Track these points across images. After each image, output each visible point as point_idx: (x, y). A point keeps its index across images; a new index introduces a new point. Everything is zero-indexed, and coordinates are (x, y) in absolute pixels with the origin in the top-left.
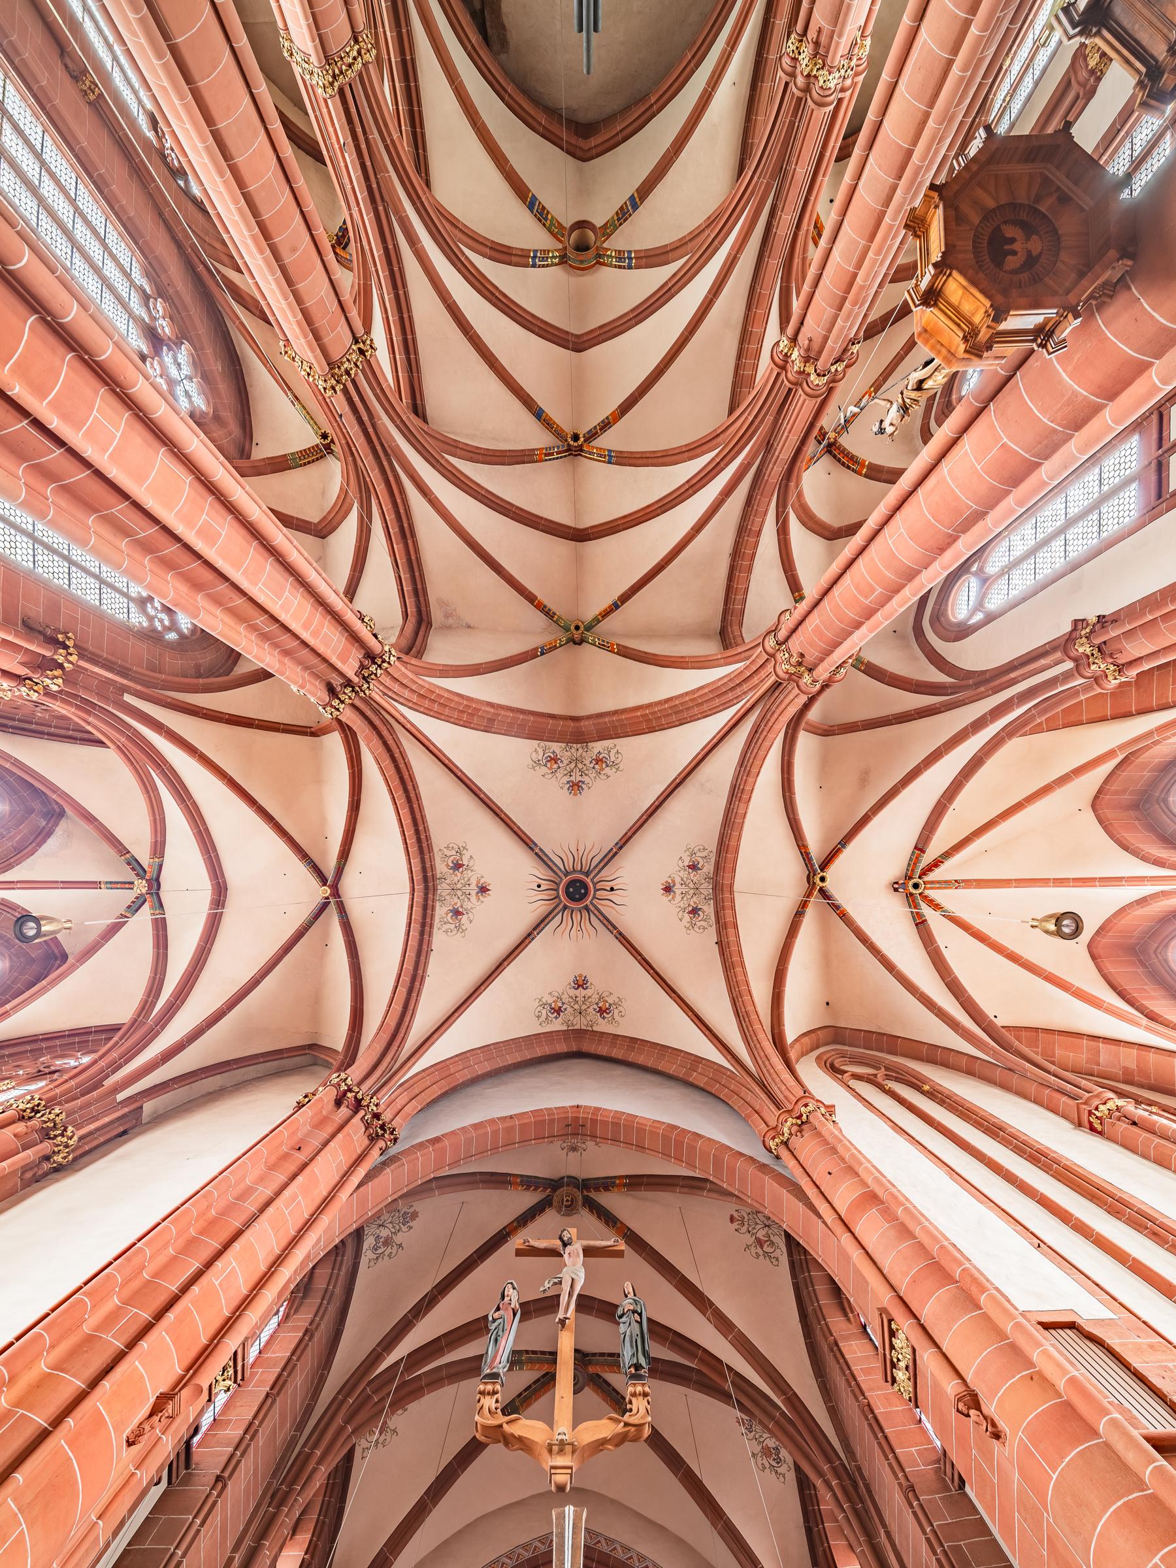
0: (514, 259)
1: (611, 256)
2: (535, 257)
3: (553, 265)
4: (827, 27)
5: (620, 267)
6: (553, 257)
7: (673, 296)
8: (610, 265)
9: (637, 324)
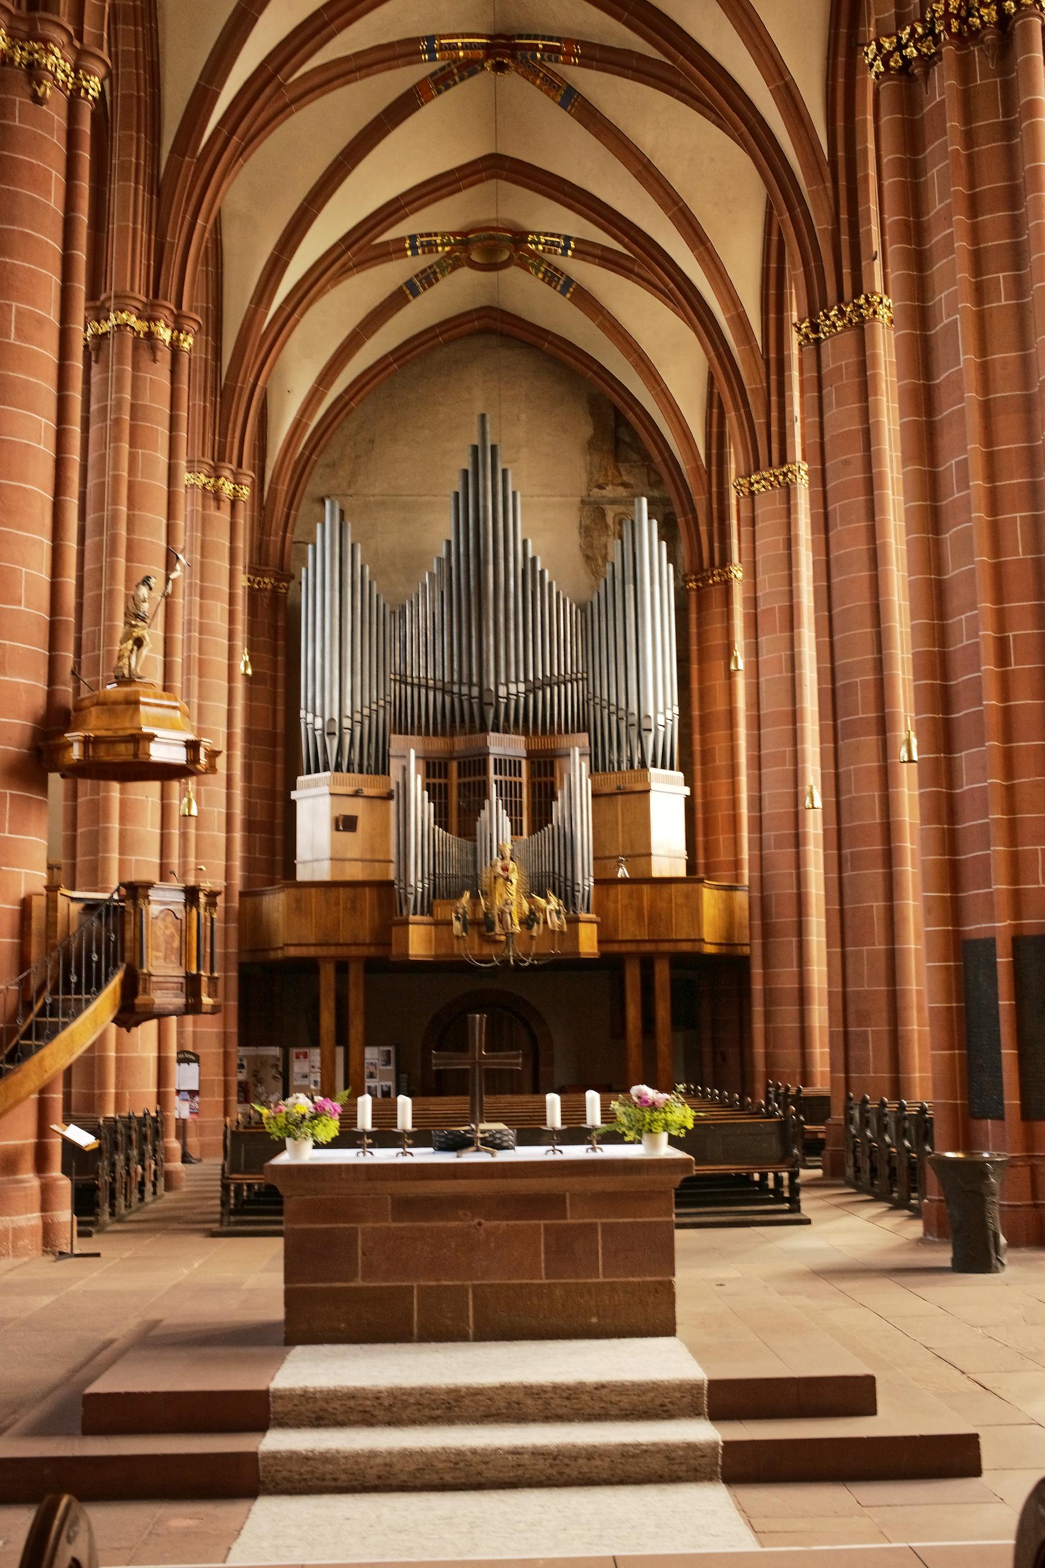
0: (599, 252)
1: (443, 245)
2: (566, 248)
3: (538, 234)
4: (212, 511)
5: (429, 235)
6: (537, 243)
7: (343, 239)
8: (443, 235)
9: (396, 199)
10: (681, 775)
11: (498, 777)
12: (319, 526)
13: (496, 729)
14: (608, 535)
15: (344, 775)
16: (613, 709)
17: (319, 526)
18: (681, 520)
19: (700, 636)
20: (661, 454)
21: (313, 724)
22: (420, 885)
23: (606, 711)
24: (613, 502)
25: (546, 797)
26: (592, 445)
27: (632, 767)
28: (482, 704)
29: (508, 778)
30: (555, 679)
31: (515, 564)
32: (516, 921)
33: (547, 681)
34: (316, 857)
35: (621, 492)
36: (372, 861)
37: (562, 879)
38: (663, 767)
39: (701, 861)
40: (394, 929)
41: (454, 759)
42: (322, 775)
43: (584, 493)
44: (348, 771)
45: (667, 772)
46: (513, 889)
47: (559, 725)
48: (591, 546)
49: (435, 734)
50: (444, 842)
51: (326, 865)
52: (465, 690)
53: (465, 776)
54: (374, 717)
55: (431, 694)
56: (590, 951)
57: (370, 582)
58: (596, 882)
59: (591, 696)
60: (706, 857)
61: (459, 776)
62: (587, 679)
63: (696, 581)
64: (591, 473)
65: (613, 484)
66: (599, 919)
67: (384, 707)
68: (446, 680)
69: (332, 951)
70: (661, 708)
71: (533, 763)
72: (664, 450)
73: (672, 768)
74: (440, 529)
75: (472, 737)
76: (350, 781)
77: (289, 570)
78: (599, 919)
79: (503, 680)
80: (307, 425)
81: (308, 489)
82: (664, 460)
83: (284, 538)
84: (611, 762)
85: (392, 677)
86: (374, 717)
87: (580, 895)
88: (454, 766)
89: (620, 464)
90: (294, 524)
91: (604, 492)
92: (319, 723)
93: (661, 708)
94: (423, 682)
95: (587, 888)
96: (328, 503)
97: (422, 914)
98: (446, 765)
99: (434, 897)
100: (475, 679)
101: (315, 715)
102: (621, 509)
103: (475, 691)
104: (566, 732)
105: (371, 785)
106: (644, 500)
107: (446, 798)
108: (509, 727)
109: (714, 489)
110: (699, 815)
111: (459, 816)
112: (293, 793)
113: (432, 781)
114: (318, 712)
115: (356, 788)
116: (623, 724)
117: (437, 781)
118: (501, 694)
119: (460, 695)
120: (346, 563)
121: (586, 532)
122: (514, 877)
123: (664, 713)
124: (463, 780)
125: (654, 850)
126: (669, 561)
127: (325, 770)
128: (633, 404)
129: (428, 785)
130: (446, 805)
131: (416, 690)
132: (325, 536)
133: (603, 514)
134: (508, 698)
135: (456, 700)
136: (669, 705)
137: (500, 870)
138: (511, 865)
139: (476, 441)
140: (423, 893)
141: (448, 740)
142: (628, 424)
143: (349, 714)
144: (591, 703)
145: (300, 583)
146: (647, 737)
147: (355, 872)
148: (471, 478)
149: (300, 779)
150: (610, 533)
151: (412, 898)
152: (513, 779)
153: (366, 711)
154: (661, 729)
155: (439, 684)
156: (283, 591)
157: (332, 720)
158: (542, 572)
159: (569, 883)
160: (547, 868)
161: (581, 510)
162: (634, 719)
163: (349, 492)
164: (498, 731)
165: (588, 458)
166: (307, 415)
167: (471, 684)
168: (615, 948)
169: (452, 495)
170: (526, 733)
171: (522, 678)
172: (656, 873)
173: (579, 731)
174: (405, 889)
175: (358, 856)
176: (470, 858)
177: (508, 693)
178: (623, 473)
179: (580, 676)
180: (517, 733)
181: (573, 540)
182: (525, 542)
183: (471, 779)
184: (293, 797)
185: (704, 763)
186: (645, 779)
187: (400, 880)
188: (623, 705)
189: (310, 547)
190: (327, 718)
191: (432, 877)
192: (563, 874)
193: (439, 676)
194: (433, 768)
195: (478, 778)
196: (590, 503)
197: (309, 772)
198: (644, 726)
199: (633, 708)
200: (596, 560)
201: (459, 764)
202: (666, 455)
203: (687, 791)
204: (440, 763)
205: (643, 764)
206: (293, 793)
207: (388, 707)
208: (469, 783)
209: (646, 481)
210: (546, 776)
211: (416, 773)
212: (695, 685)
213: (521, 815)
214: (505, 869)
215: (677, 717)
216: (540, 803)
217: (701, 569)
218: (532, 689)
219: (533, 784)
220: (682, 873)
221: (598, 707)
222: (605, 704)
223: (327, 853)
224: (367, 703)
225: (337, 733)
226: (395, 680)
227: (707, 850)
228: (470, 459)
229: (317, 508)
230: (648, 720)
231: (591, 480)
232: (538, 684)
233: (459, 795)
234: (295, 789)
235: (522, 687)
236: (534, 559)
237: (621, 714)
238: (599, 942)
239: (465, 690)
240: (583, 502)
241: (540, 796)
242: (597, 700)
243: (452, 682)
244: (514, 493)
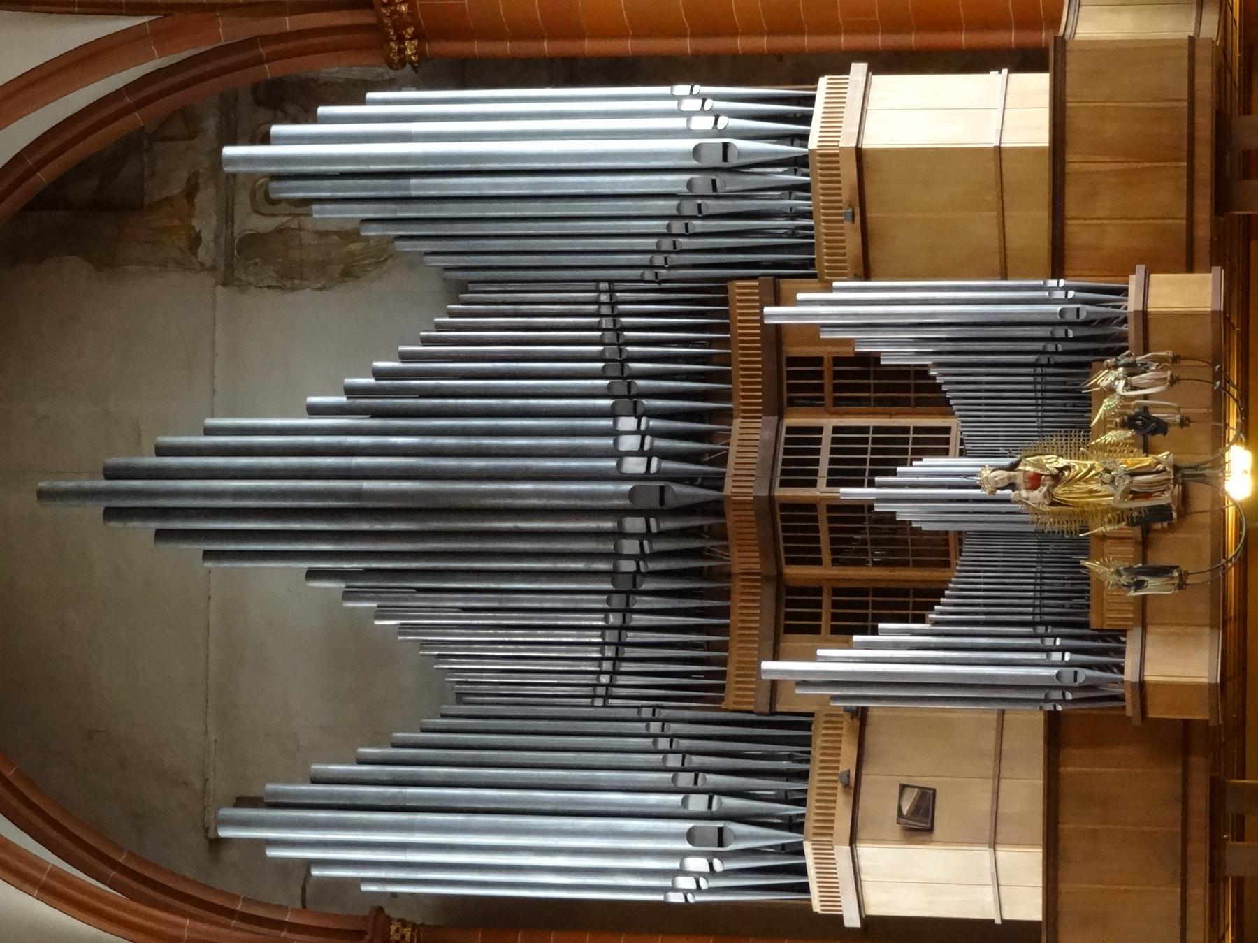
10: (823, 81)
11: (822, 480)
12: (272, 853)
13: (716, 482)
14: (300, 229)
15: (811, 812)
16: (678, 227)
17: (272, 853)
18: (269, 71)
19: (520, 34)
20: (127, 111)
21: (697, 875)
22: (1056, 656)
23: (684, 242)
24: (228, 217)
25: (865, 375)
26: (107, 261)
27: (805, 187)
28: (663, 511)
29: (825, 457)
30: (611, 352)
31: (361, 432)
32: (1148, 460)
33: (614, 369)
34: (988, 879)
35: (206, 197)
36: (999, 756)
37: (1051, 347)
38: (806, 119)
39: (1012, 38)
40: (1152, 714)
41: (780, 574)
42: (810, 860)
43: (207, 280)
44: (801, 802)
45: (818, 110)
46: (1080, 466)
47: (711, 343)
48: (321, 268)
49: (724, 612)
50: (965, 599)
51: (1004, 854)
52: (630, 546)
53: (819, 551)
54: (685, 744)
55: (639, 620)
56: (1209, 290)
57: (394, 746)
58: (1056, 275)
59: (649, 275)
60: (1004, 26)
61: (818, 562)
62: (610, 281)
63: (401, 39)
64: (163, 264)
65: (190, 215)
66: (1141, 269)
67: (664, 721)
68: (609, 587)
69: (1199, 848)
70: (679, 123)
71: (791, 402)
72: (121, 105)
73: (810, 101)
74: (286, 595)
75: (732, 532)
76: (824, 800)
77: (365, 918)
78: (1141, 269)
79: (612, 463)
80: (55, 874)
81: (188, 872)
82: (139, 105)
83: (293, 928)
84: (793, 233)
85: (599, 702)
86: (685, 744)
87: (1086, 310)
88: (796, 572)
89: (146, 200)
90: (268, 906)
91: (207, 237)
92: (698, 864)
93: (679, 123)
94: (611, 636)
95: (1071, 294)
96: (224, 833)
97: (1121, 652)
98: (792, 590)
99: (1086, 625)
100: (608, 525)
101: (682, 872)
102: (243, 198)
103: (635, 524)
104: (724, 328)
105: (833, 753)
106: (229, 151)
107: (863, 592)
108: (712, 452)
110: (912, 40)
111: (905, 564)
112: (848, 924)
113: (825, 623)
114: (675, 865)
115: (840, 786)
116: (712, 206)
117: (826, 611)
118: (642, 469)
119: (641, 557)
120: (355, 795)
121: (290, 276)
122: (1054, 462)
123: (689, 115)
124: (826, 556)
125: (991, 141)
126: (362, 101)
127: (801, 853)
128: (20, 170)
129: (835, 630)
130: (878, 592)
131: (629, 652)
132: (292, 840)
134: (649, 455)
135: (653, 566)
136: (672, 105)
137: (1037, 495)
138: (1027, 468)
139: (96, 509)
140: (1074, 651)
141: (737, 585)
142: (60, 182)
143: (678, 798)
144: (663, 273)
145: (394, 895)
146: (741, 154)
147: (1025, 792)
148: (173, 522)
149: (817, 907)
150: (294, 225)
151: (1084, 674)
152: (826, 446)
153: (674, 761)
154: (723, 122)
155: (618, 601)
156: (408, 932)
157: (690, 836)
158: (379, 374)
159: (1060, 332)
160: (1025, 379)
161: (243, 287)
162: (702, 182)
163: (198, 785)
164: (721, 477)
165: (133, 268)
166: (35, 873)
167: (620, 534)
168: (1203, 232)
169: (209, 565)
170: (725, 416)
171: (608, 423)
172: (1040, 137)
173: (724, 302)
174: (1064, 689)
175: (989, 785)
176: (1000, 545)
177: (640, 453)
178: (166, 193)
179: (604, 298)
180: (727, 435)
181: (312, 308)
182: (314, 411)
183: (824, 536)
184: (858, 924)
185: (798, 31)
186: (830, 159)
187: (1047, 700)
188: (669, 206)
189: (315, 872)
190: (686, 846)
191: (1041, 630)
192: (1038, 346)
193: (599, 602)
194: (801, 617)
195: (823, 525)
196: (230, 267)
197: (805, 888)
198: (717, 161)
199: (676, 182)
200: (353, 254)
201: (790, 562)
202: (128, 100)
203: (859, 69)
204: (789, 604)
205: (799, 163)
206: (848, 924)
207: (664, 713)
208: (833, 541)
209: (183, 144)
210: (819, 375)
211: (813, 658)
212: (629, 46)
213: (905, 430)
214: (1035, 481)
215: (698, 89)
216: (878, 388)
217: (376, 28)
218: (631, 401)
219: (838, 402)
220: (1039, 83)
221: (674, 259)
222: (666, 244)
223: (984, 854)
224: (655, 759)
225: (720, 824)
226: (607, 697)
227: (987, 25)
228: (135, 524)
229: (230, 855)
230: (703, 152)
231: (180, 265)
232: (620, 387)
233: (861, 563)
234: (840, 918)
235: (628, 423)
236: (351, 392)
237: (689, 208)
238: (1190, 268)
239: (630, 546)
240: (225, 284)
241: (866, 388)
242: (659, 260)
243: (613, 574)
244: (209, 431)
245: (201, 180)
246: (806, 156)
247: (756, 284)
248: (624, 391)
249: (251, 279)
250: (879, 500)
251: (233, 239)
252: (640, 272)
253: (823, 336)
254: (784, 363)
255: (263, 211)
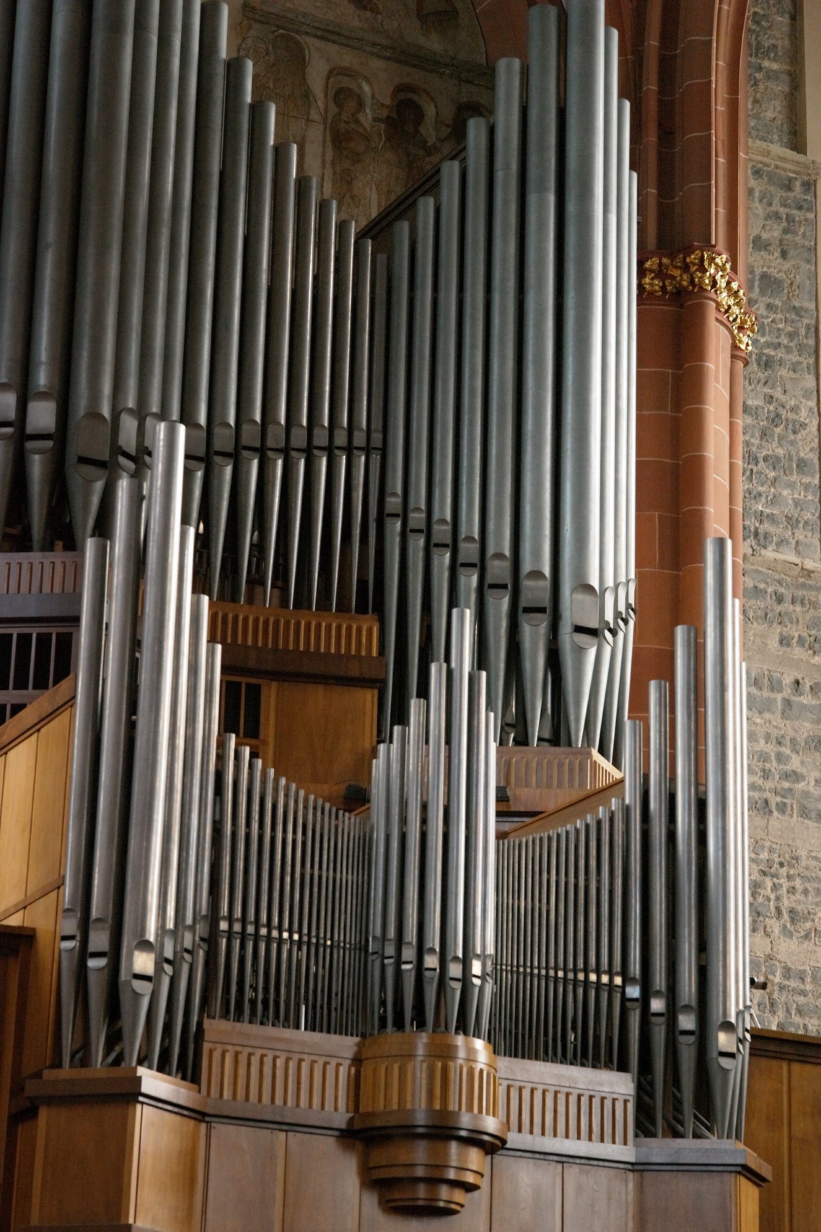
24: (329, 34)
79: (131, 403)
102: (347, 59)
109: (653, 42)
133: (299, 61)
146: (580, 651)
150: (314, 115)
174: (115, 954)
176: (347, 876)
191: (202, 929)
232: (223, 440)
245: (369, 14)
246: (570, 744)
247: (375, 653)
248: (217, 446)
249: (249, 42)
250: (450, 672)
251: (298, 32)
252: (399, 490)
253: (680, 632)
254: (253, 681)
255: (332, 79)
